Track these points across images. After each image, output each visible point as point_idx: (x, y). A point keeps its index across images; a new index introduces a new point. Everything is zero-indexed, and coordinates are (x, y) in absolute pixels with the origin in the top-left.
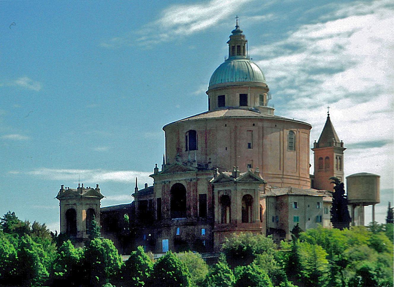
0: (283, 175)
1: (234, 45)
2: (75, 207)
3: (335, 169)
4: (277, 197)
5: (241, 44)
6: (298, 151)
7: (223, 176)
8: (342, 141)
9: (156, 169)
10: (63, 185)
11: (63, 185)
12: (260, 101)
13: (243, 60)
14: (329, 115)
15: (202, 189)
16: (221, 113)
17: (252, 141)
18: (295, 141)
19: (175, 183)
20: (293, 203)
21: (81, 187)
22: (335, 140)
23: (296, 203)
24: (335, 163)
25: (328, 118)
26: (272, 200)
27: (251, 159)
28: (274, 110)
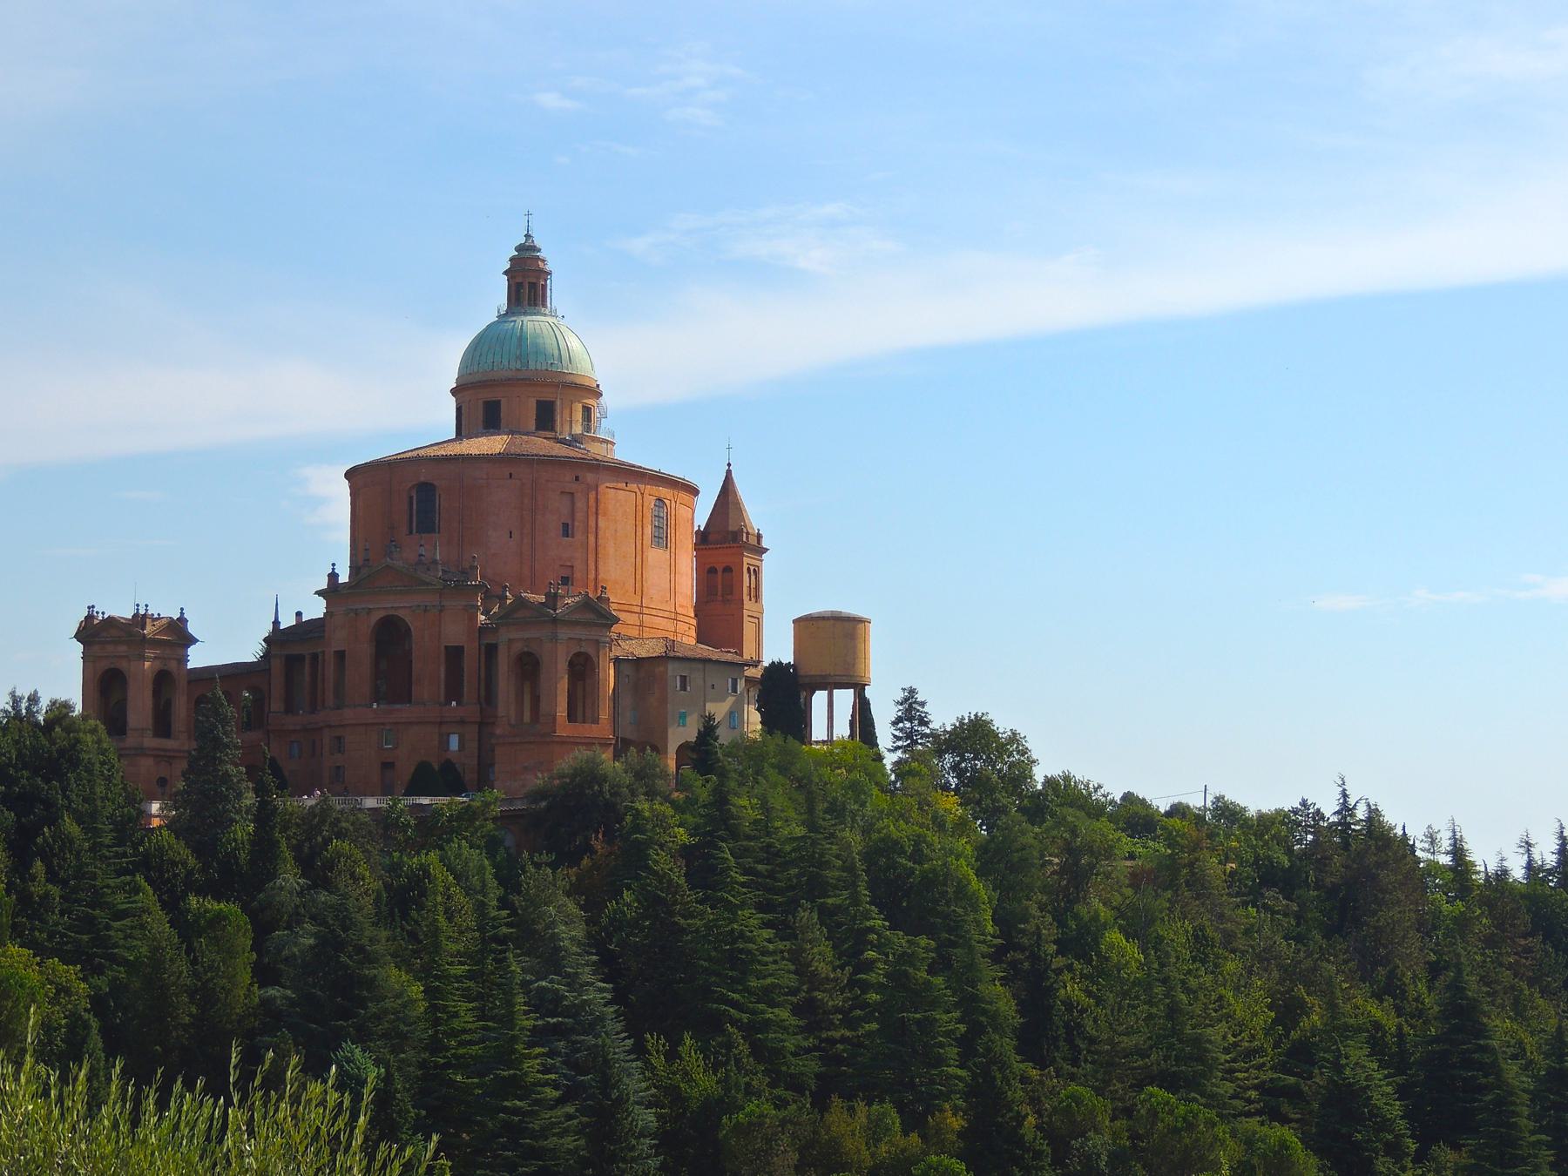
0: (642, 606)
1: (520, 281)
2: (123, 665)
3: (746, 598)
4: (639, 661)
5: (538, 278)
6: (673, 550)
7: (521, 603)
8: (759, 530)
9: (333, 576)
10: (93, 607)
11: (93, 607)
12: (584, 420)
13: (542, 318)
14: (729, 465)
15: (454, 632)
16: (493, 444)
17: (573, 520)
18: (667, 525)
19: (382, 614)
20: (678, 678)
21: (142, 612)
22: (745, 526)
23: (685, 677)
24: (746, 584)
25: (729, 472)
26: (627, 670)
27: (569, 564)
28: (613, 444)
